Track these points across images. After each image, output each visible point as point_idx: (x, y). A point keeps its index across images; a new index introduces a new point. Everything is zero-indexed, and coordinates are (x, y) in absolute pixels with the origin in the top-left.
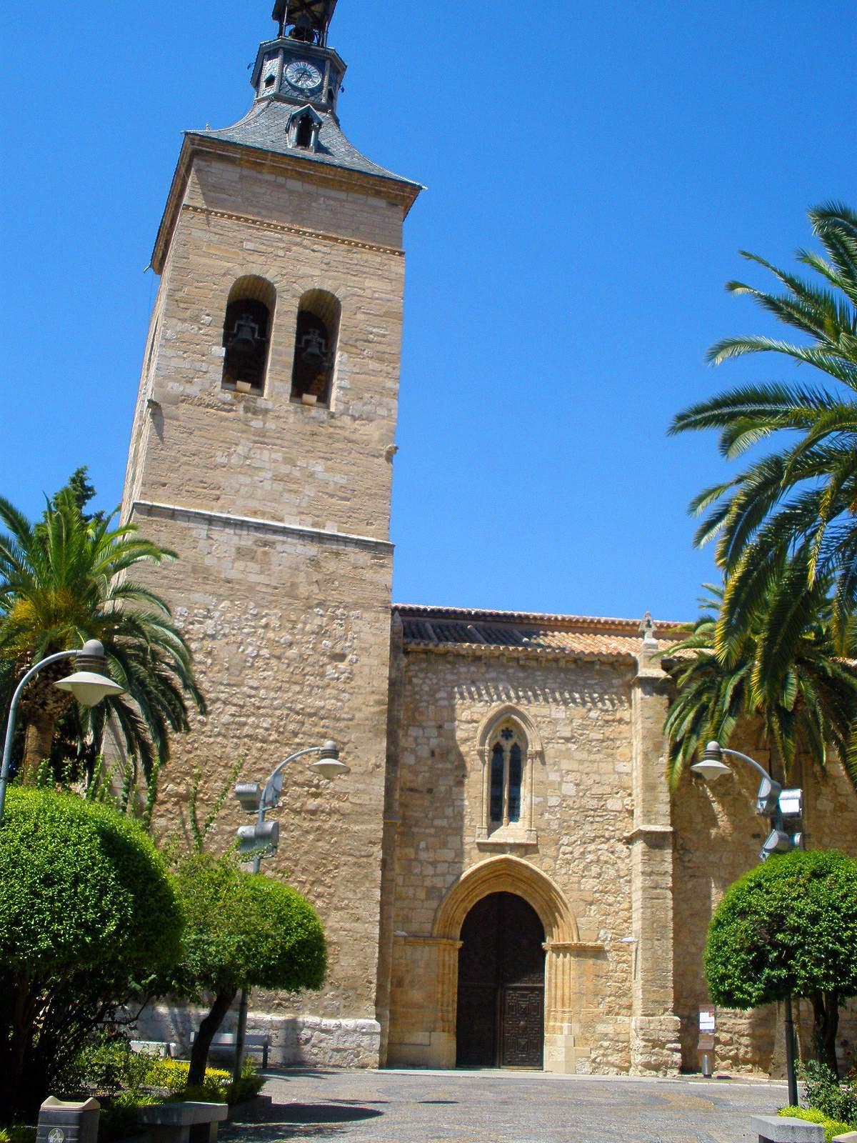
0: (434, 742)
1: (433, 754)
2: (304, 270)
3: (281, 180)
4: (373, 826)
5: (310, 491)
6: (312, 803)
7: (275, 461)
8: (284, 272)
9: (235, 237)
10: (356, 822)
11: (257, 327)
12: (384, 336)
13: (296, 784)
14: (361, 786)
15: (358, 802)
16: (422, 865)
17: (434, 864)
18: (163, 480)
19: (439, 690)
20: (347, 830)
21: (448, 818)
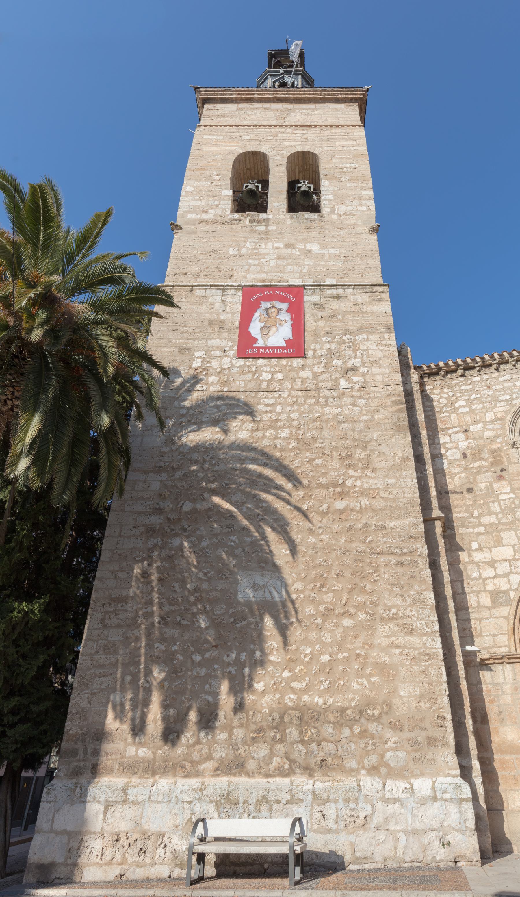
0: (463, 445)
1: (465, 456)
2: (286, 144)
3: (266, 105)
4: (414, 520)
5: (309, 262)
6: (340, 505)
7: (278, 248)
8: (273, 146)
10: (391, 518)
12: (356, 168)
13: (320, 486)
14: (391, 481)
15: (391, 496)
16: (478, 566)
17: (492, 564)
18: (185, 271)
19: (457, 400)
20: (383, 527)
21: (496, 514)
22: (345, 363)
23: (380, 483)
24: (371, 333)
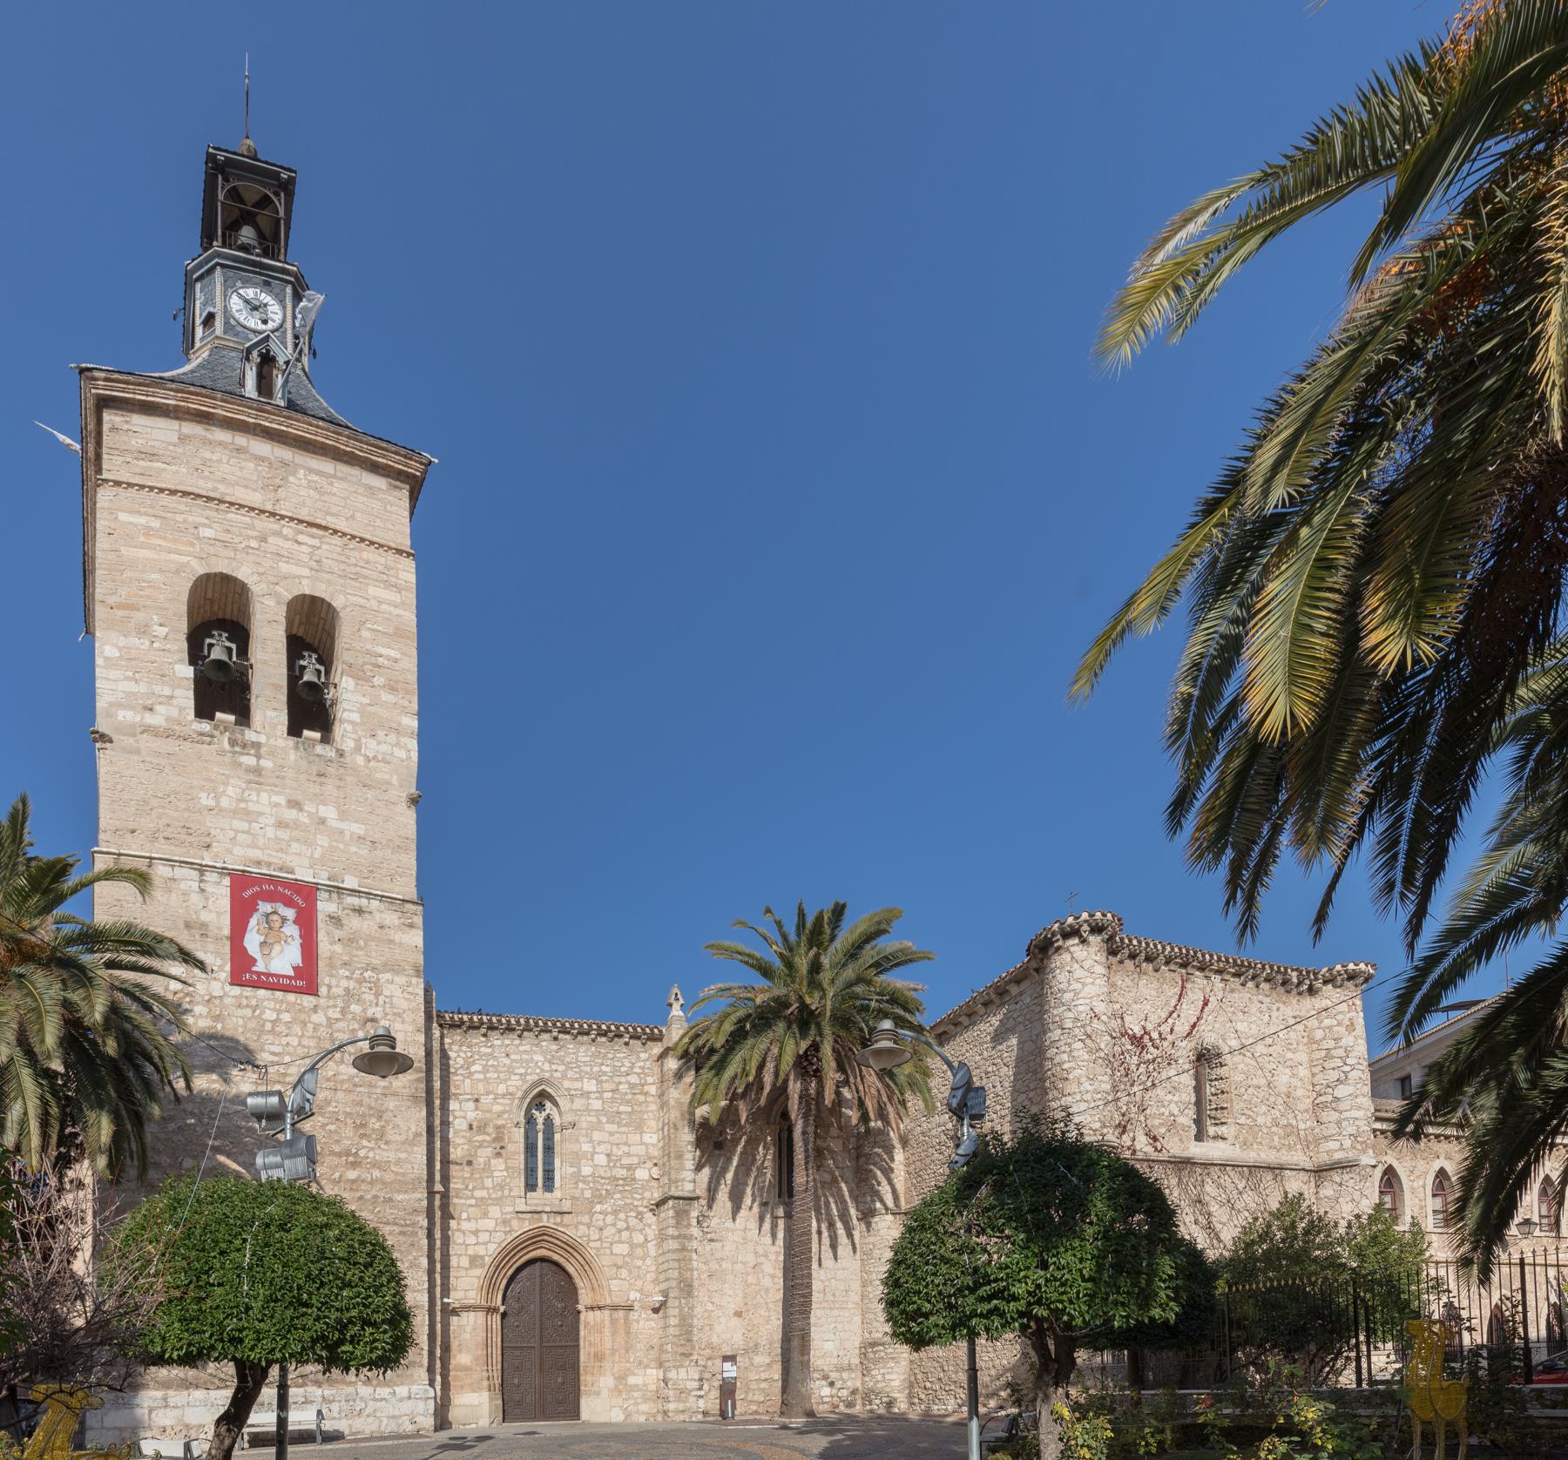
2: (285, 568)
5: (322, 841)
8: (261, 570)
9: (185, 521)
11: (234, 646)
22: (364, 1010)
23: (390, 1155)
24: (397, 973)
